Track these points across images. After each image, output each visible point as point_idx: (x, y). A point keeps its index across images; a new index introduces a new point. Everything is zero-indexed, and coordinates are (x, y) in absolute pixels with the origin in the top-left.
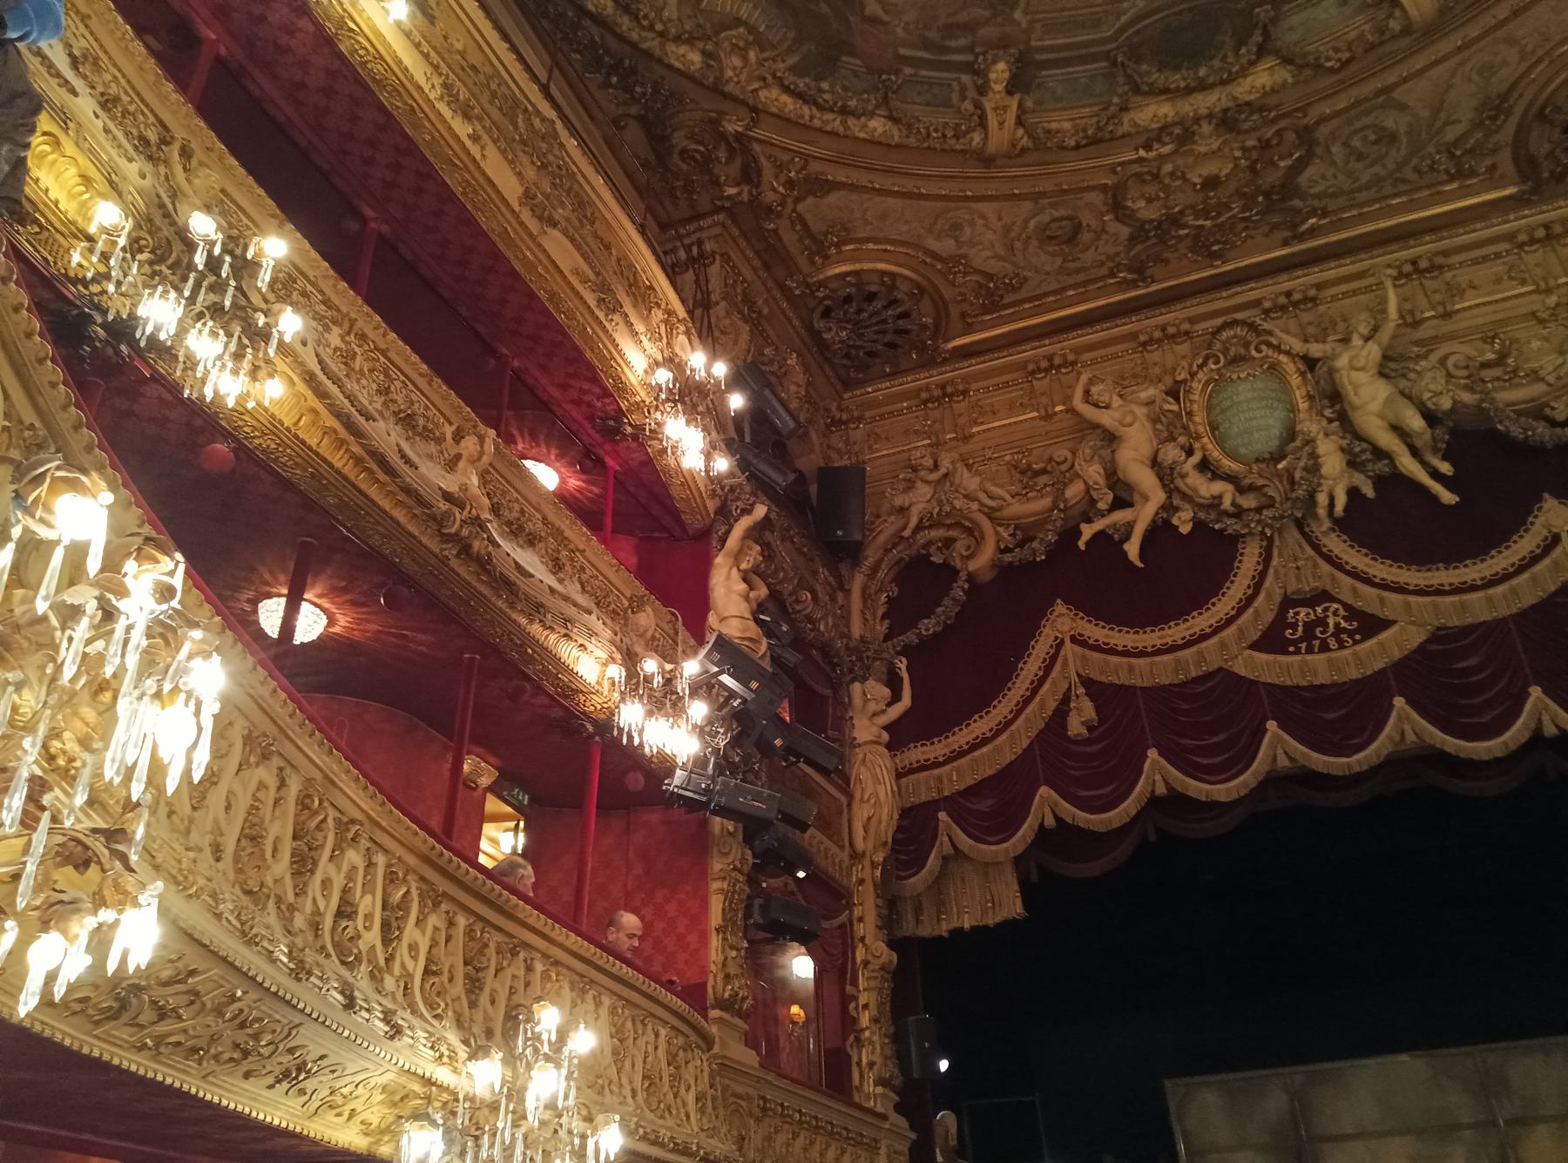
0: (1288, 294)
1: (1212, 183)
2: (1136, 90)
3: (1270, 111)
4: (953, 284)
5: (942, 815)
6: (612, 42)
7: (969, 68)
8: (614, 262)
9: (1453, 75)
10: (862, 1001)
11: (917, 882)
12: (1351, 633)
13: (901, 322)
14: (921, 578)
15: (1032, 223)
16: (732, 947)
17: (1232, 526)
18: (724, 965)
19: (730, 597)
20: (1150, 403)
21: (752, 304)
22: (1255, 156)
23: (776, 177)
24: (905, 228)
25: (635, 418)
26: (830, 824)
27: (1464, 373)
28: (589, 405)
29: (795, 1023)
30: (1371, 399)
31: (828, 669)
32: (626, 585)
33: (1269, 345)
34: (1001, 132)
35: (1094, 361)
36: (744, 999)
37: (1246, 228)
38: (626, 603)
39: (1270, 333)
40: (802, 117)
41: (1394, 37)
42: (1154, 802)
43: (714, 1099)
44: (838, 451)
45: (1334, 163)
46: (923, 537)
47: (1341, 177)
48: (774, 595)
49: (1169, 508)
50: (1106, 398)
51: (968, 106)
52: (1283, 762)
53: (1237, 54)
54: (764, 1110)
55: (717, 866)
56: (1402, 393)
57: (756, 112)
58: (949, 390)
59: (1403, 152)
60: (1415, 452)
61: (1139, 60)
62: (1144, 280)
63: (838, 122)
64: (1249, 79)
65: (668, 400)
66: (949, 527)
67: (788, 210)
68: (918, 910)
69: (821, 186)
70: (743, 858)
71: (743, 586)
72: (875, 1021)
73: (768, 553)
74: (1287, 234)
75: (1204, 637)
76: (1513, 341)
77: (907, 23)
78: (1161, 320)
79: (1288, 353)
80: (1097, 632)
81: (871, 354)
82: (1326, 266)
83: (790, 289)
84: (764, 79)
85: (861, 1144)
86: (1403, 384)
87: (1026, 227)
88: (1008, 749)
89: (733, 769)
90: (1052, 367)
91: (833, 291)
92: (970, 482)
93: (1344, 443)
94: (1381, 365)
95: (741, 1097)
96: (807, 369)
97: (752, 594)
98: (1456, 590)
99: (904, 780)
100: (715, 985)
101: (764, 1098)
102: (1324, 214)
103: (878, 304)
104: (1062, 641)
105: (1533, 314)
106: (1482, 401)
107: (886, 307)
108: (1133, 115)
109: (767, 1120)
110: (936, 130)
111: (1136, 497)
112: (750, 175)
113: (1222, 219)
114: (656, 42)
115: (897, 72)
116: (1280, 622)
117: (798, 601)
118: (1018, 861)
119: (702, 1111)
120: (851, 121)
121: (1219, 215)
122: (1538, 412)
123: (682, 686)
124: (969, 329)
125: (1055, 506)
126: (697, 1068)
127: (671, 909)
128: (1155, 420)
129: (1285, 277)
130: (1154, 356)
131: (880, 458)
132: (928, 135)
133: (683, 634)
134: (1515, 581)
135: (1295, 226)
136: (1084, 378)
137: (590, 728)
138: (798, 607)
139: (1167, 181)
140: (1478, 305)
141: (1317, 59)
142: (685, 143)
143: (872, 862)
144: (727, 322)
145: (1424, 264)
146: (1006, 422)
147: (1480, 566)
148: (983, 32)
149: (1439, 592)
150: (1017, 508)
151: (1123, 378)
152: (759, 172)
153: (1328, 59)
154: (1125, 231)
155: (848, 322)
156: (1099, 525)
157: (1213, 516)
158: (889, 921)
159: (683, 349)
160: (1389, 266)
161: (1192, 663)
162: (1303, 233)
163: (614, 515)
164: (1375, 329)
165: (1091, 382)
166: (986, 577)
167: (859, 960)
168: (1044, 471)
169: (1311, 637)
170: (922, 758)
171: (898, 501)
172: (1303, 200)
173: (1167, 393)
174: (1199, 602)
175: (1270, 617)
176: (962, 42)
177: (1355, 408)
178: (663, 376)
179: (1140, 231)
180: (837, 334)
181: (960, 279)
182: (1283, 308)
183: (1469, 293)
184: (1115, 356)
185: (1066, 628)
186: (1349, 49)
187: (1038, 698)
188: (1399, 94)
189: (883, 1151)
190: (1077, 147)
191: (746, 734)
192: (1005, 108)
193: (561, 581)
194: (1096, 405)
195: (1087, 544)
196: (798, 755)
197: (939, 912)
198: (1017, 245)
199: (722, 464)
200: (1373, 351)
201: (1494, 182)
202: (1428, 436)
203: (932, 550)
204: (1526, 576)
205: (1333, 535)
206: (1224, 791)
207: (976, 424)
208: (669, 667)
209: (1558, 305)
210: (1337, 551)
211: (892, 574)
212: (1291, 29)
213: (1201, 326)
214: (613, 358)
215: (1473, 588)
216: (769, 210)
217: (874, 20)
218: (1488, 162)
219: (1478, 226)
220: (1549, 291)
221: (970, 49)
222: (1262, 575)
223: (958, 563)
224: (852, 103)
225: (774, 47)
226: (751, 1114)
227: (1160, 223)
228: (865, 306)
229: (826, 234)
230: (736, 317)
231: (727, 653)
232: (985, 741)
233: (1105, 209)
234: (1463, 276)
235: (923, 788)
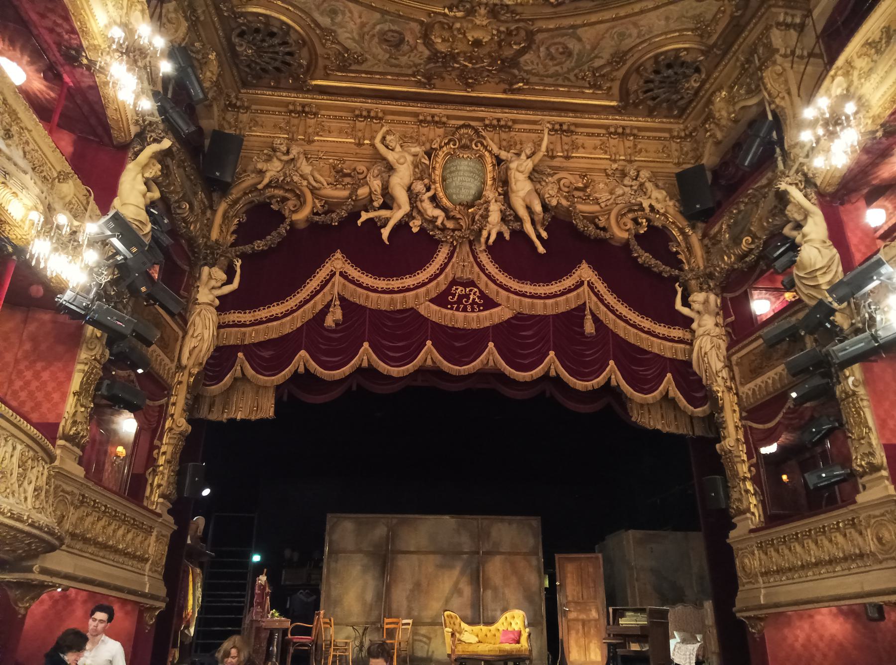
0: (499, 120)
1: (477, 43)
3: (517, 14)
4: (324, 45)
5: (240, 355)
9: (605, 33)
10: (163, 449)
11: (215, 389)
12: (479, 306)
13: (288, 58)
14: (261, 216)
15: (378, 27)
16: (82, 406)
17: (439, 235)
18: (74, 414)
19: (133, 192)
20: (415, 155)
21: (194, 11)
22: (503, 37)
25: (91, 55)
26: (169, 345)
27: (566, 190)
28: (59, 35)
29: (118, 457)
30: (521, 188)
31: (190, 254)
32: (58, 162)
33: (482, 144)
35: (392, 122)
36: (83, 437)
37: (488, 76)
38: (55, 175)
39: (484, 138)
42: (360, 370)
43: (47, 491)
44: (229, 123)
45: (539, 57)
46: (270, 192)
47: (540, 66)
48: (164, 198)
49: (410, 216)
50: (393, 144)
52: (429, 362)
54: (82, 502)
55: (83, 355)
56: (536, 191)
58: (307, 109)
59: (573, 64)
60: (533, 223)
62: (430, 85)
65: (117, 50)
66: (287, 191)
68: (211, 406)
70: (103, 355)
71: (144, 188)
72: (168, 462)
73: (166, 171)
74: (507, 87)
75: (408, 289)
76: (593, 181)
78: (433, 111)
79: (490, 152)
80: (354, 273)
81: (264, 70)
82: (520, 112)
83: (221, 9)
85: (142, 528)
86: (538, 186)
87: (374, 28)
88: (287, 326)
89: (109, 298)
90: (369, 116)
92: (306, 169)
93: (503, 208)
94: (531, 173)
95: (67, 493)
96: (220, 65)
97: (149, 194)
98: (532, 296)
99: (222, 330)
100: (65, 425)
101: (83, 496)
102: (527, 83)
103: (276, 41)
104: (335, 273)
105: (605, 170)
106: (570, 206)
109: (82, 508)
111: (395, 205)
113: (478, 66)
116: (447, 292)
117: (179, 207)
118: (278, 388)
119: (37, 497)
121: (477, 63)
122: (592, 219)
123: (82, 238)
124: (327, 77)
125: (350, 197)
126: (39, 473)
127: (45, 375)
128: (416, 166)
129: (499, 110)
130: (424, 130)
131: (256, 136)
133: (93, 205)
134: (558, 299)
135: (511, 84)
136: (384, 129)
137: (10, 249)
138: (179, 211)
139: (455, 33)
140: (582, 157)
143: (190, 373)
144: (173, 15)
145: (565, 127)
146: (335, 139)
147: (546, 288)
149: (524, 295)
150: (329, 192)
151: (405, 137)
154: (427, 53)
155: (254, 45)
156: (371, 215)
157: (431, 227)
158: (191, 408)
160: (549, 122)
161: (399, 302)
162: (515, 89)
163: (61, 115)
164: (533, 154)
165: (388, 132)
166: (302, 226)
167: (166, 427)
168: (349, 175)
169: (460, 304)
170: (237, 320)
171: (259, 166)
172: (519, 71)
173: (426, 153)
174: (411, 271)
175: (444, 287)
177: (513, 192)
178: (118, 33)
179: (435, 56)
180: (245, 50)
181: (329, 44)
182: (494, 127)
183: (581, 150)
184: (404, 123)
185: (338, 267)
187: (312, 302)
188: (580, 31)
189: (155, 533)
191: (123, 280)
193: (8, 146)
194: (387, 147)
195: (362, 223)
196: (156, 301)
197: (224, 408)
198: (367, 37)
199: (147, 105)
200: (529, 165)
201: (609, 97)
202: (541, 216)
203: (274, 201)
204: (564, 297)
205: (485, 254)
206: (396, 371)
207: (318, 135)
208: (76, 223)
209: (617, 169)
210: (484, 262)
211: (244, 209)
213: (453, 122)
214: (83, 8)
215: (539, 297)
218: (608, 85)
219: (595, 116)
220: (615, 161)
222: (446, 265)
223: (287, 213)
226: (72, 504)
227: (446, 55)
228: (267, 38)
231: (121, 225)
232: (277, 318)
233: (419, 35)
234: (580, 140)
235: (232, 337)
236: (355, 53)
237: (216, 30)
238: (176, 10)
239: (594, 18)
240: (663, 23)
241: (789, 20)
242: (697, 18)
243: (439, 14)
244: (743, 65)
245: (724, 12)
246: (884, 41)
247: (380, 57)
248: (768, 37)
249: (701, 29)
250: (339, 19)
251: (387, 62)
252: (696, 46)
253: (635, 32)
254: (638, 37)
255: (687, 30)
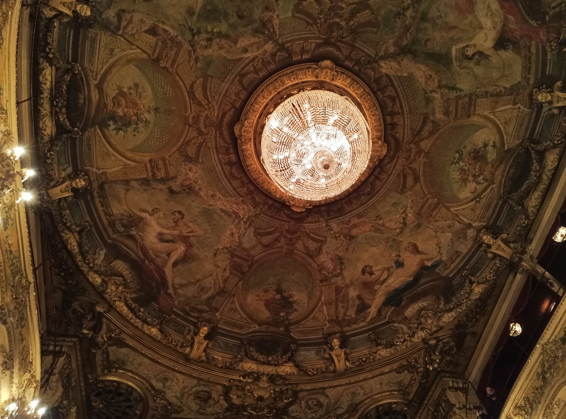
1: (261, 398)
2: (246, 355)
3: (287, 380)
4: (155, 401)
6: (70, 262)
7: (195, 324)
8: (21, 348)
9: (344, 392)
13: (127, 409)
15: (194, 389)
22: (277, 394)
23: (106, 333)
24: (146, 372)
34: (197, 352)
40: (128, 317)
41: (330, 372)
45: (301, 407)
47: (302, 413)
51: (189, 337)
53: (282, 357)
57: (111, 307)
61: (251, 345)
63: (140, 324)
64: (284, 367)
67: (104, 348)
69: (121, 344)
77: (180, 301)
83: (89, 379)
84: (120, 298)
91: (106, 386)
103: (122, 399)
107: (124, 401)
108: (243, 364)
110: (175, 342)
112: (96, 329)
114: (87, 269)
115: (169, 315)
120: (145, 326)
121: (259, 412)
132: (171, 342)
141: (307, 370)
142: (77, 307)
144: (54, 384)
148: (204, 315)
152: (101, 329)
153: (310, 371)
154: (226, 405)
159: (29, 395)
176: (196, 315)
180: (98, 405)
186: (317, 371)
188: (327, 391)
190: (221, 367)
192: (202, 343)
198: (185, 395)
212: (300, 355)
216: (96, 345)
217: (169, 295)
221: (197, 318)
224: (149, 320)
225: (130, 289)
227: (239, 406)
229: (114, 362)
230: (60, 385)
233: (222, 394)
236: (176, 406)
237: (81, 391)
238: (57, 381)
239: (335, 383)
240: (379, 386)
241: (456, 385)
242: (398, 383)
243: (237, 380)
244: (433, 413)
245: (415, 380)
246: (528, 406)
247: (193, 408)
248: (446, 396)
249: (403, 390)
250: (169, 384)
251: (198, 412)
252: (401, 401)
253: (362, 392)
254: (364, 395)
255: (394, 391)
